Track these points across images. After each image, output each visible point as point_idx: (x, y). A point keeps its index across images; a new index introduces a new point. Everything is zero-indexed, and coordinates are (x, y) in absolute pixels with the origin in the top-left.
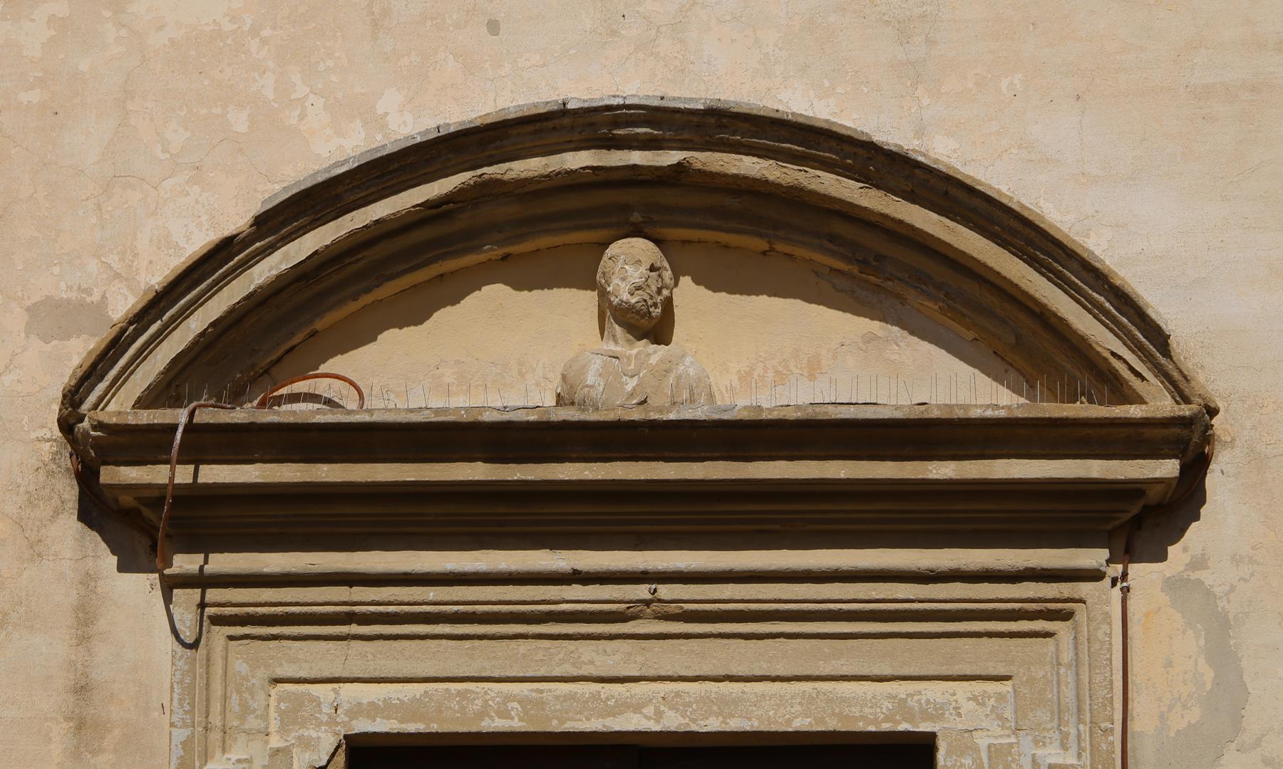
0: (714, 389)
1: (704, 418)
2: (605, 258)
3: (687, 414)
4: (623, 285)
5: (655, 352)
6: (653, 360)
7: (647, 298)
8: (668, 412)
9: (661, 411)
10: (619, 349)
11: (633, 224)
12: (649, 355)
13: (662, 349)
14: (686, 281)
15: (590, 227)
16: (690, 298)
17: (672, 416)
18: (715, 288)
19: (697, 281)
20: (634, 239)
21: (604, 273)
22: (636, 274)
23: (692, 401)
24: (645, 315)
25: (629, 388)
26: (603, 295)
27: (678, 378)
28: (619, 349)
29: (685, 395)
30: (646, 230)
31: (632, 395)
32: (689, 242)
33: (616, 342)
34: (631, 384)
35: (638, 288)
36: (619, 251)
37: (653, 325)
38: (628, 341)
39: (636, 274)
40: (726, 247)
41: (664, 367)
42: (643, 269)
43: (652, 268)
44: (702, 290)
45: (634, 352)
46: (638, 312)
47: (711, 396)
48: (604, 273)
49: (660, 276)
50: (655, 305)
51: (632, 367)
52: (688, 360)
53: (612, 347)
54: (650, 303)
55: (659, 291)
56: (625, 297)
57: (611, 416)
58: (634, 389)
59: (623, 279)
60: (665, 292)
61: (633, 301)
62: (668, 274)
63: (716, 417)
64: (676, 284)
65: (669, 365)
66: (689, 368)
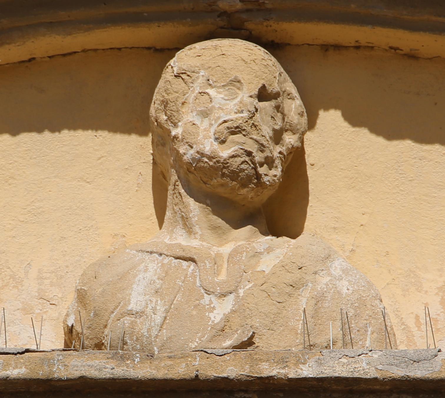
0: (392, 320)
1: (372, 374)
2: (167, 75)
3: (338, 367)
4: (203, 124)
5: (269, 250)
6: (267, 264)
7: (253, 147)
8: (299, 362)
9: (283, 361)
10: (195, 243)
11: (223, 14)
12: (257, 255)
13: (283, 243)
14: (331, 119)
15: (136, 19)
16: (340, 151)
17: (308, 371)
18: (391, 134)
19: (354, 119)
20: (226, 43)
21: (165, 103)
22: (231, 106)
23: (347, 341)
24: (249, 179)
25: (216, 317)
26: (164, 142)
27: (318, 300)
28: (195, 243)
29: (333, 331)
30: (250, 25)
31: (222, 331)
32: (338, 47)
33: (189, 229)
34: (220, 310)
35: (236, 131)
36: (195, 62)
37: (266, 200)
38: (214, 228)
39: (232, 105)
40: (412, 56)
41: (289, 278)
42: (245, 96)
43: (263, 95)
44: (364, 135)
45: (227, 249)
46: (234, 175)
47: (386, 335)
48: (165, 103)
49: (278, 108)
50: (269, 162)
51: (223, 276)
52: (337, 266)
53: (180, 239)
54: (259, 157)
55: (277, 137)
56: (209, 146)
57: (181, 371)
58: (227, 319)
59: (205, 114)
60: (290, 139)
61: (225, 153)
62: (294, 106)
63: (398, 372)
64: (311, 125)
65: (298, 274)
66: (339, 280)
